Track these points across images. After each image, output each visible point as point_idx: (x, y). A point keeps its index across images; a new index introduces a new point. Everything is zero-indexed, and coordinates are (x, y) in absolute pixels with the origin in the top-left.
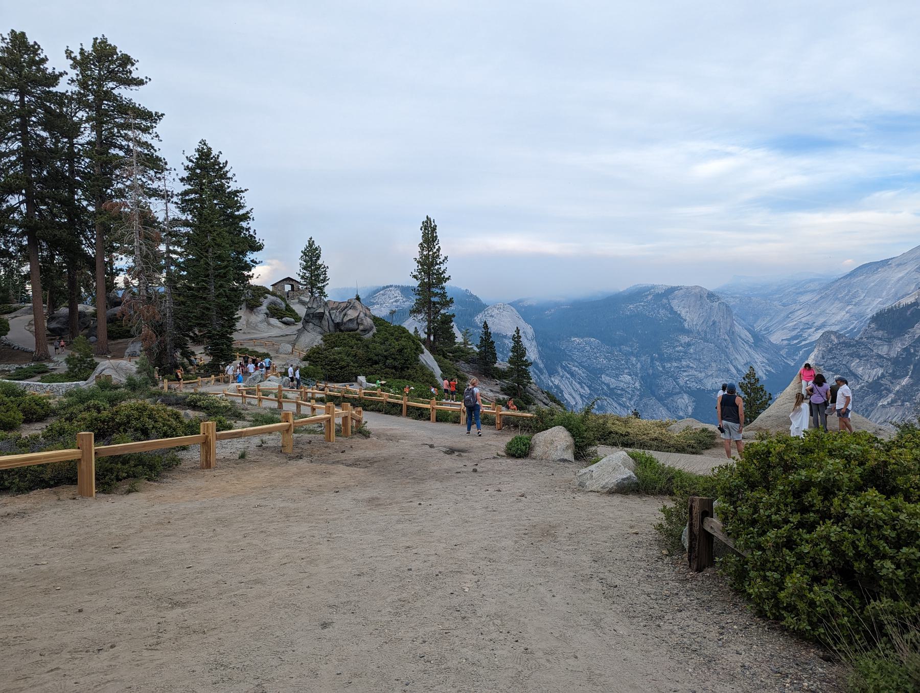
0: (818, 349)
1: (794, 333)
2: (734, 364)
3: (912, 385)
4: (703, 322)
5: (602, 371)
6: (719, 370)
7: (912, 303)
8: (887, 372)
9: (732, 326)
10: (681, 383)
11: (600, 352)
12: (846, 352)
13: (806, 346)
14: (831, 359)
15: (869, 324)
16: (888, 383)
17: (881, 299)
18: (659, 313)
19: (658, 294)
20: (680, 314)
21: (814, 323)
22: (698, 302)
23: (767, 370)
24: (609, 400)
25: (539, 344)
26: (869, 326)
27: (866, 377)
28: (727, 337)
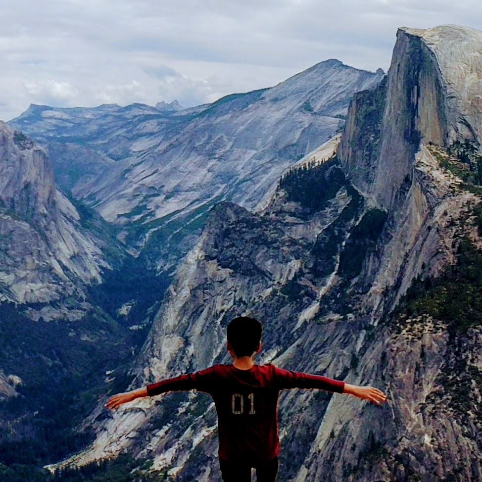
0: (209, 232)
1: (136, 202)
2: (58, 258)
3: (341, 285)
4: (8, 185)
7: (329, 159)
8: (306, 267)
9: (51, 193)
12: (248, 237)
14: (227, 247)
15: (277, 190)
16: (309, 284)
17: (254, 152)
21: (163, 186)
23: (101, 267)
26: (277, 195)
28: (45, 212)
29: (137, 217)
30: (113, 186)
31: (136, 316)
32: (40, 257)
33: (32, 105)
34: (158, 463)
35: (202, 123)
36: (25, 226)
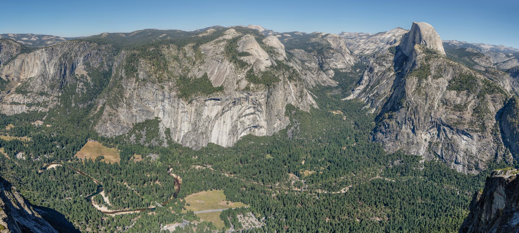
5: (305, 61)
6: (342, 62)
10: (331, 66)
13: (364, 55)
19: (323, 36)
20: (330, 43)
24: (308, 71)
25: (286, 51)
29: (361, 54)
30: (356, 48)
31: (360, 72)
34: (362, 100)
35: (374, 37)
36: (340, 54)
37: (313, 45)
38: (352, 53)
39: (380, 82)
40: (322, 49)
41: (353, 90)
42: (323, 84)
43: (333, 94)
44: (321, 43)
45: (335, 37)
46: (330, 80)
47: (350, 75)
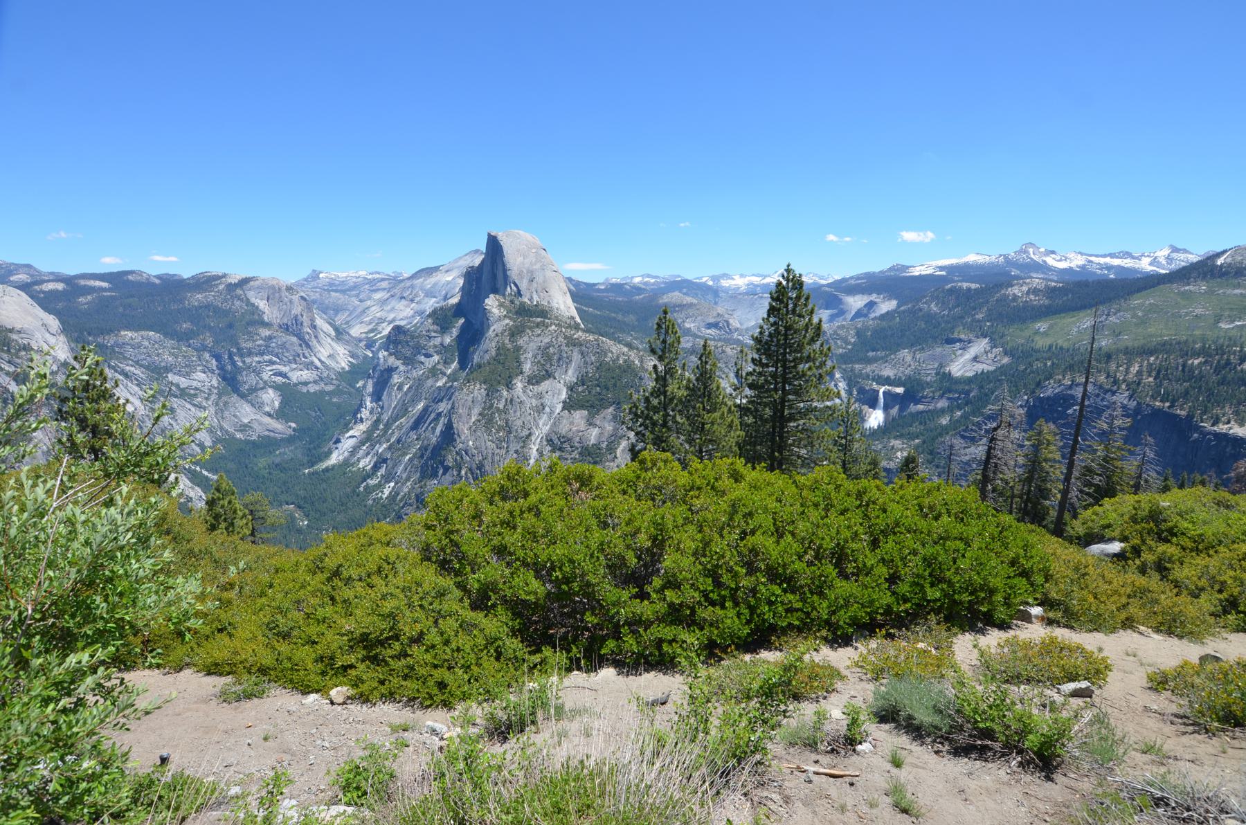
1: (371, 327)
5: (168, 369)
9: (313, 320)
10: (265, 376)
11: (164, 348)
13: (381, 338)
18: (233, 304)
19: (230, 284)
20: (257, 307)
22: (277, 295)
27: (427, 364)
30: (358, 317)
32: (306, 358)
33: (314, 271)
34: (361, 465)
35: (408, 284)
36: (294, 339)
37: (197, 315)
38: (340, 334)
39: (410, 409)
40: (231, 326)
41: (338, 441)
42: (239, 435)
43: (278, 460)
44: (226, 306)
45: (273, 287)
46: (267, 420)
47: (335, 400)
